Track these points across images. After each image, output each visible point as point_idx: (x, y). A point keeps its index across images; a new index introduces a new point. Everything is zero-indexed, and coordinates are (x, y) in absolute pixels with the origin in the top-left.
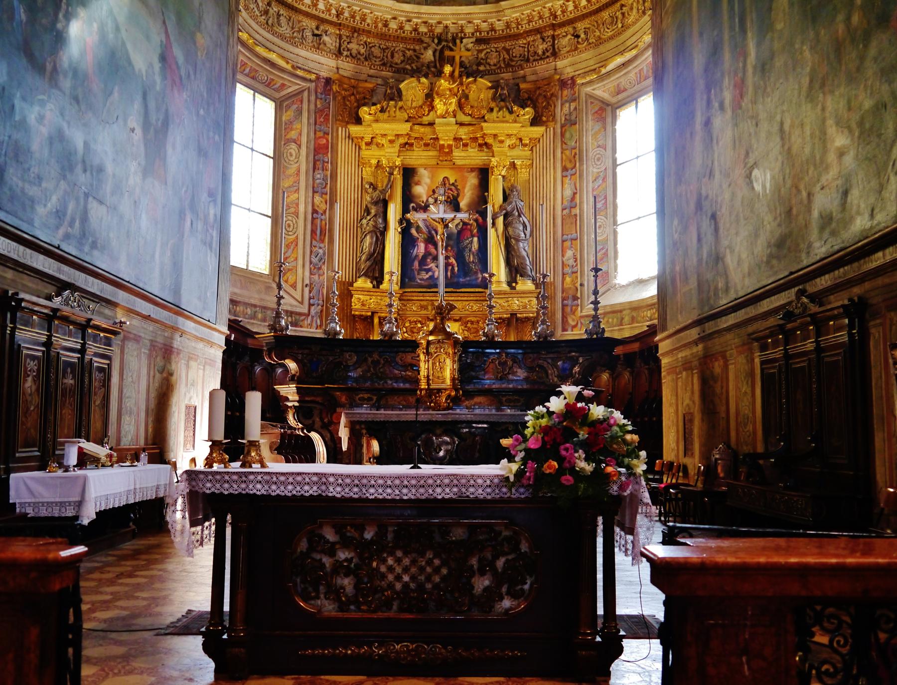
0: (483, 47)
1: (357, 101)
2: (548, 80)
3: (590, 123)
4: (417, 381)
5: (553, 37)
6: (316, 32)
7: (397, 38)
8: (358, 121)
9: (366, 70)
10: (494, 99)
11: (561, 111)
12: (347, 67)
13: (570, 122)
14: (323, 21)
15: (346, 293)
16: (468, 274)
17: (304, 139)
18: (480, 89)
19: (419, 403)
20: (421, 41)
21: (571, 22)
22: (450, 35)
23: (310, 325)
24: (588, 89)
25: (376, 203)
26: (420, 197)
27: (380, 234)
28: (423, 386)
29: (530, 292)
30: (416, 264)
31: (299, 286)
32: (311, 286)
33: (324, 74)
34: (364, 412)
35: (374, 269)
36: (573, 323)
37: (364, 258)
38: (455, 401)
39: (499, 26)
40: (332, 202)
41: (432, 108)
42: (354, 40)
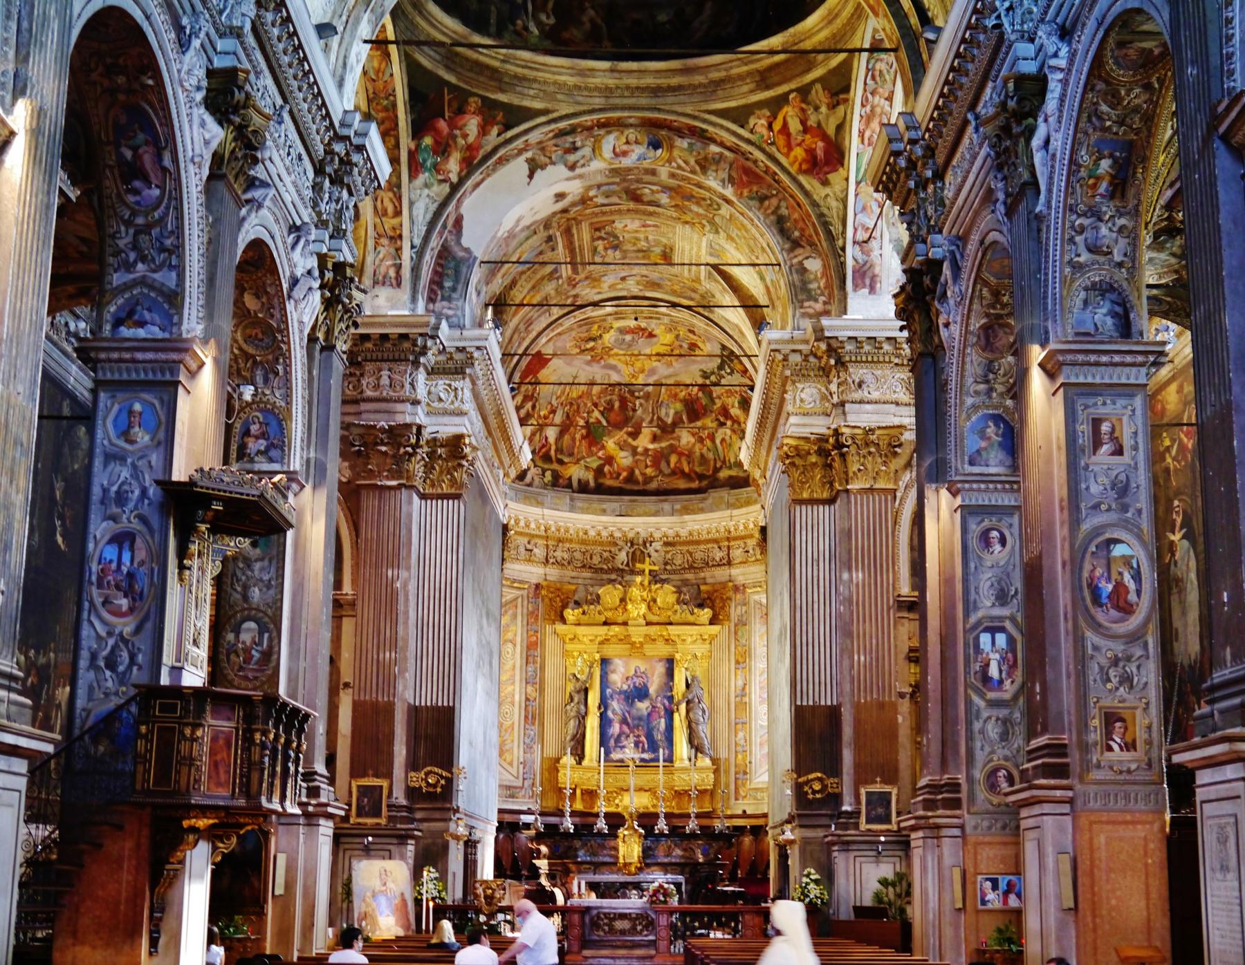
0: (669, 548)
1: (562, 601)
2: (724, 585)
3: (758, 626)
4: (617, 858)
5: (729, 548)
6: (529, 547)
7: (595, 543)
8: (563, 620)
9: (569, 573)
10: (678, 602)
11: (735, 611)
12: (553, 573)
13: (742, 623)
14: (533, 536)
15: (553, 766)
16: (656, 745)
17: (519, 639)
18: (666, 595)
19: (619, 870)
20: (616, 544)
21: (742, 538)
22: (641, 541)
23: (524, 796)
24: (756, 597)
25: (578, 692)
26: (615, 683)
27: (582, 718)
28: (621, 861)
29: (708, 768)
30: (612, 742)
31: (515, 764)
32: (524, 763)
33: (534, 581)
34: (592, 877)
35: (579, 755)
36: (743, 794)
37: (568, 738)
38: (640, 870)
39: (684, 533)
40: (542, 691)
41: (626, 610)
42: (559, 550)
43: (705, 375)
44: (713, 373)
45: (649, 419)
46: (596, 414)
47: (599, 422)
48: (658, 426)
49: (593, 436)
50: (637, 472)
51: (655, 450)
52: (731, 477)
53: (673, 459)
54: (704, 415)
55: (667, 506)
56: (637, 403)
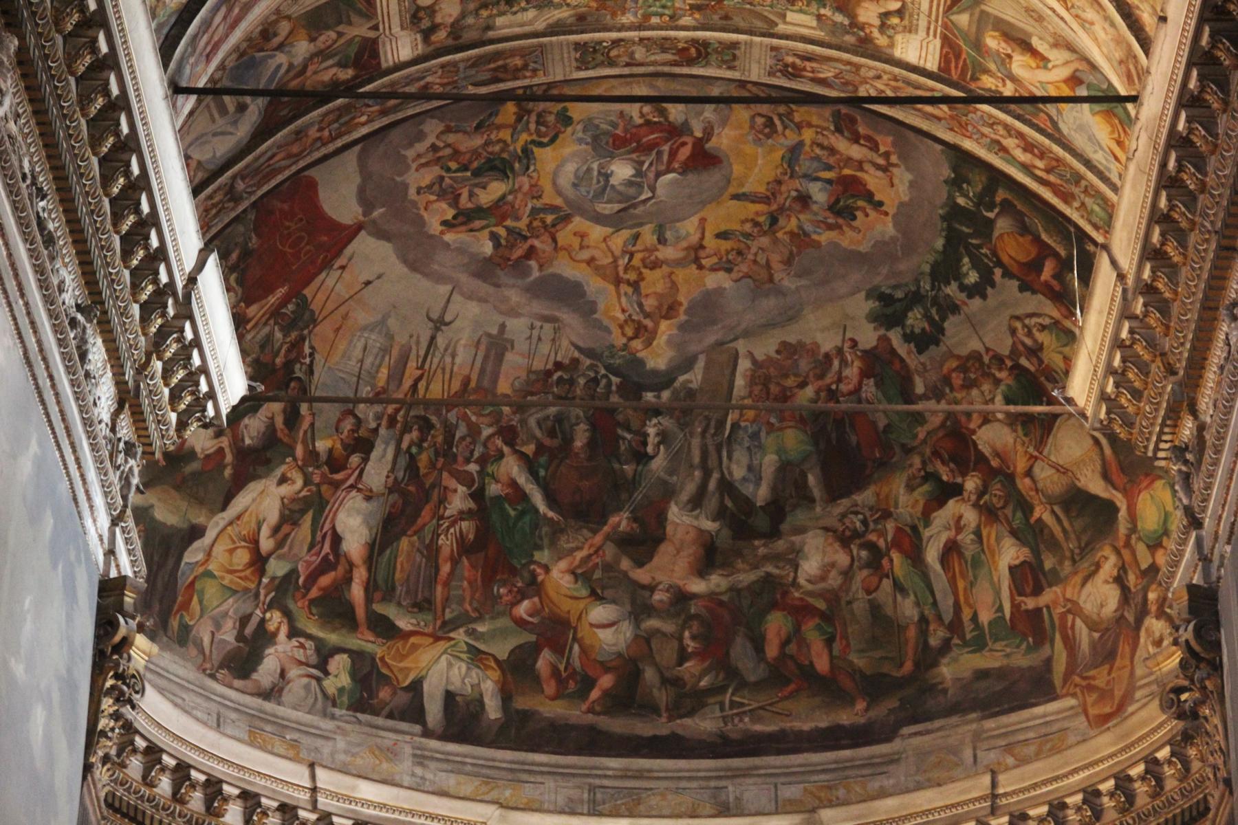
43: (889, 311)
44: (915, 298)
45: (690, 488)
46: (511, 468)
47: (519, 495)
48: (720, 514)
49: (499, 549)
50: (650, 674)
51: (712, 596)
52: (982, 674)
53: (776, 625)
54: (885, 466)
55: (752, 791)
56: (651, 431)
